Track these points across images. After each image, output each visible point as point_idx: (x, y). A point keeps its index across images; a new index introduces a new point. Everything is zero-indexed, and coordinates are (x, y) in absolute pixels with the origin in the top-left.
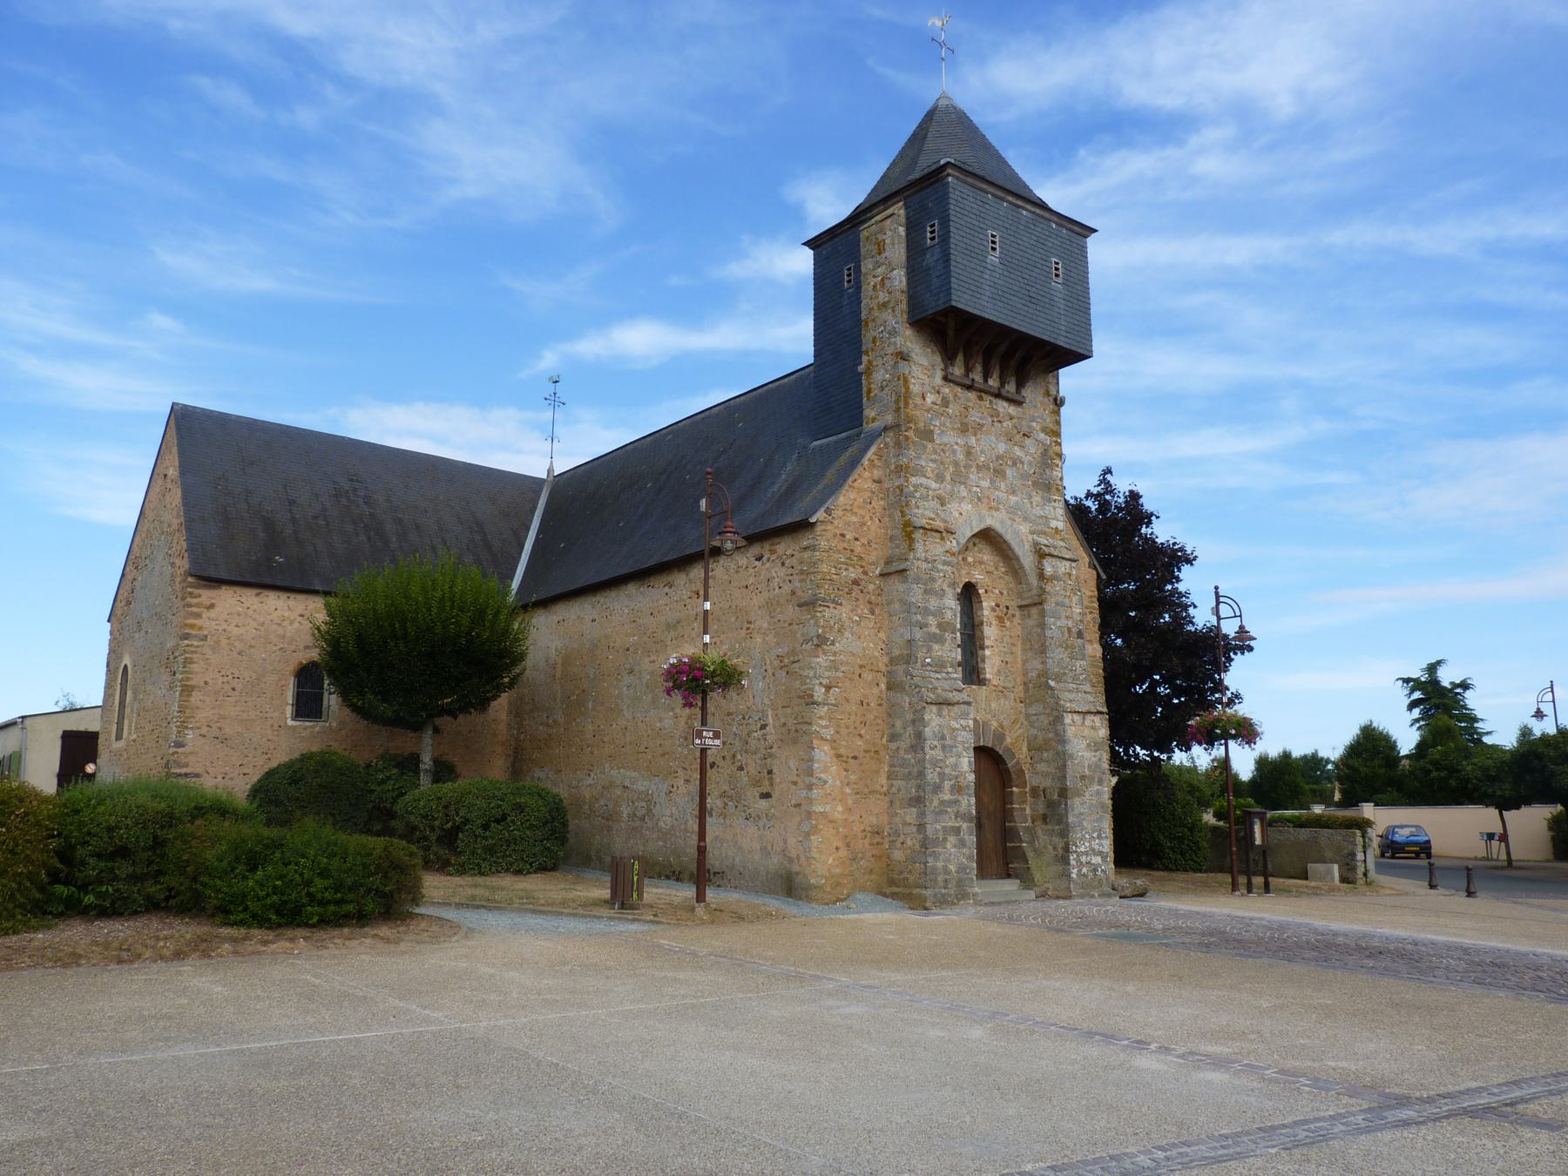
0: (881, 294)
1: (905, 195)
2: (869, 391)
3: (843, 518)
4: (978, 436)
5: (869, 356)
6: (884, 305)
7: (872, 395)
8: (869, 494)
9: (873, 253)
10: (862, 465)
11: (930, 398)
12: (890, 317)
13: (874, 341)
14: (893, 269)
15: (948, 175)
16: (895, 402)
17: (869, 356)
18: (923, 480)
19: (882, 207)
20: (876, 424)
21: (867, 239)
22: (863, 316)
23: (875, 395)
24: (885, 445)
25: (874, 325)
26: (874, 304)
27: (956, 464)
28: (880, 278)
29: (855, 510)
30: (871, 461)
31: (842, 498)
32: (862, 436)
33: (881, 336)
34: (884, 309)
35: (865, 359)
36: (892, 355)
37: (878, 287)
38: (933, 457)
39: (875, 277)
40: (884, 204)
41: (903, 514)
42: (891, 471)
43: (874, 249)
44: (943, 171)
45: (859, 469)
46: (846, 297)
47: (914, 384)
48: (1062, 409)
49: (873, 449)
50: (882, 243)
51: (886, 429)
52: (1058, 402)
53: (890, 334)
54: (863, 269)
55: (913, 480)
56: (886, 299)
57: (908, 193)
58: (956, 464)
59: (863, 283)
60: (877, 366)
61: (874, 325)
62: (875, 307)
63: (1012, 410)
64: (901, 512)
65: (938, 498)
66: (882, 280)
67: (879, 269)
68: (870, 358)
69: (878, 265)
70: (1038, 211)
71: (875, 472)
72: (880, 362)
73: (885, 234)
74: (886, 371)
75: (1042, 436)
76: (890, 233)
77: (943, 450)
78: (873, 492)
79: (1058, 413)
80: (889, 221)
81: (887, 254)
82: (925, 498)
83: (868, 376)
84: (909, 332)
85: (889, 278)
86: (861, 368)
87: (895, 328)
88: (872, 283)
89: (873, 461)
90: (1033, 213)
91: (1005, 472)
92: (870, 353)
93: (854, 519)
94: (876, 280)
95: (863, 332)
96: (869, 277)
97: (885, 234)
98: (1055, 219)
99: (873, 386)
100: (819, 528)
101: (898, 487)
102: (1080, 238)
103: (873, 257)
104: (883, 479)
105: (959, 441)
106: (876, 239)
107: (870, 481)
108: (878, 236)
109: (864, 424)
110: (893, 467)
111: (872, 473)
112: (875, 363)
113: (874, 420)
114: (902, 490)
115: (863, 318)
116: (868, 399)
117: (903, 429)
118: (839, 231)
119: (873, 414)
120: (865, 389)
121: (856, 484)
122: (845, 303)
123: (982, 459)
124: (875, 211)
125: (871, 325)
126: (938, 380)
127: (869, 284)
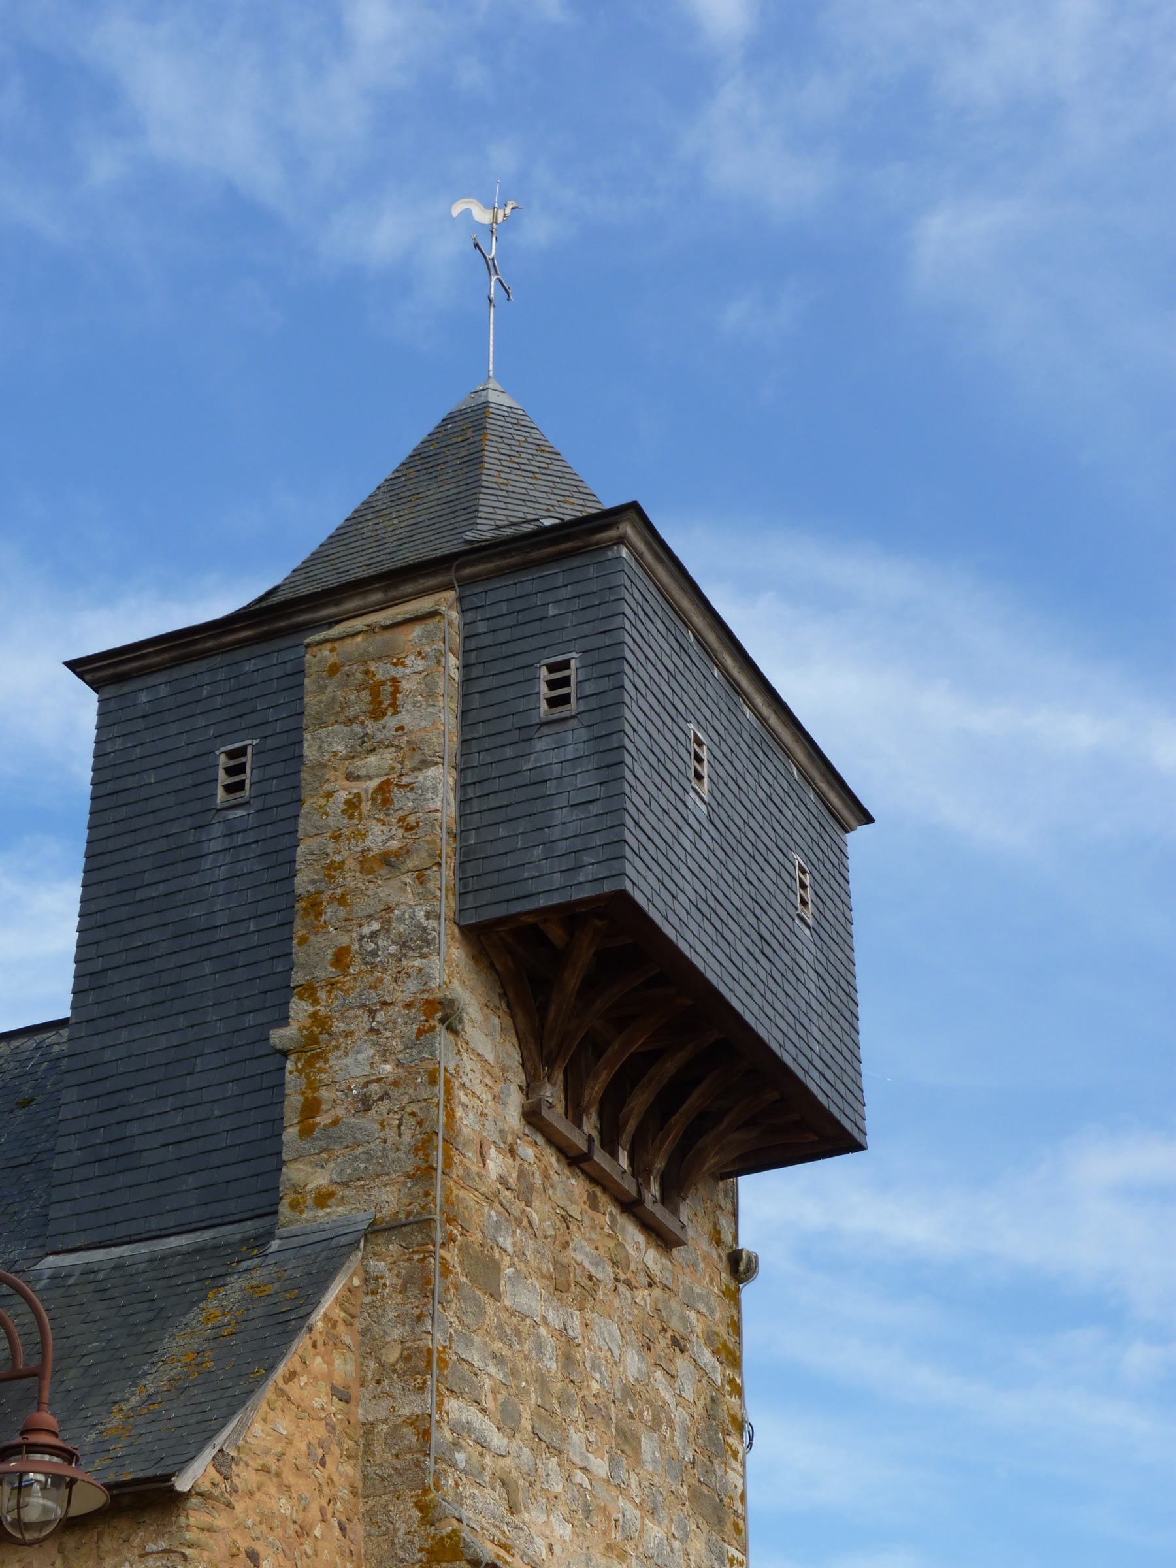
0: (377, 828)
1: (467, 571)
2: (311, 1108)
3: (258, 1495)
4: (589, 1315)
5: (316, 1002)
6: (388, 860)
7: (322, 1120)
8: (321, 1431)
9: (350, 713)
10: (310, 1330)
11: (496, 1164)
12: (409, 898)
13: (341, 958)
14: (425, 764)
15: (622, 540)
16: (416, 1150)
17: (316, 1002)
18: (471, 1414)
19: (377, 597)
20: (334, 1213)
21: (333, 670)
22: (303, 882)
23: (335, 1123)
24: (366, 1281)
25: (342, 913)
26: (346, 853)
27: (543, 1383)
28: (373, 784)
29: (289, 1477)
30: (331, 1322)
31: (257, 1428)
32: (275, 1245)
33: (371, 946)
34: (384, 871)
35: (300, 1009)
36: (408, 1006)
37: (366, 806)
38: (497, 1345)
39: (351, 777)
40: (386, 589)
41: (428, 1513)
42: (386, 1370)
43: (360, 702)
44: (607, 527)
45: (302, 1343)
46: (217, 830)
47: (465, 1106)
48: (748, 1292)
49: (336, 1288)
50: (389, 688)
51: (376, 1230)
52: (742, 1268)
53: (404, 945)
54: (310, 751)
55: (452, 1404)
56: (395, 845)
57: (480, 568)
58: (543, 1383)
59: (304, 794)
60: (349, 1034)
61: (342, 913)
62: (351, 863)
63: (652, 1258)
64: (419, 1506)
65: (504, 1483)
66: (383, 788)
67: (372, 759)
68: (322, 1009)
69: (367, 746)
70: (773, 720)
71: (338, 1362)
72: (362, 1022)
73: (400, 663)
74: (385, 1054)
75: (707, 1357)
76: (420, 664)
77: (517, 1332)
78: (331, 1428)
79: (733, 1297)
80: (417, 631)
81: (404, 718)
82: (475, 1473)
83: (309, 1063)
84: (457, 953)
85: (410, 787)
86: (280, 1036)
87: (425, 929)
88: (343, 795)
89: (334, 1325)
90: (763, 720)
91: (639, 1439)
92: (322, 994)
93: (284, 1507)
94: (356, 787)
95: (299, 930)
96: (330, 774)
97: (400, 663)
98: (801, 756)
99: (324, 1094)
100: (195, 1517)
101: (412, 1421)
102: (836, 827)
103: (350, 721)
104: (355, 1390)
105: (551, 1314)
106: (366, 672)
107: (324, 1388)
108: (373, 667)
109: (284, 1208)
110: (392, 1355)
111: (330, 1363)
112: (338, 1026)
113: (322, 1199)
114: (426, 1434)
115: (299, 891)
116: (306, 1132)
117: (439, 1237)
118: (209, 644)
119: (320, 1180)
120: (293, 1101)
121: (293, 1389)
122: (214, 846)
123: (595, 1387)
124: (351, 605)
125: (329, 912)
126: (513, 1119)
127: (329, 795)
